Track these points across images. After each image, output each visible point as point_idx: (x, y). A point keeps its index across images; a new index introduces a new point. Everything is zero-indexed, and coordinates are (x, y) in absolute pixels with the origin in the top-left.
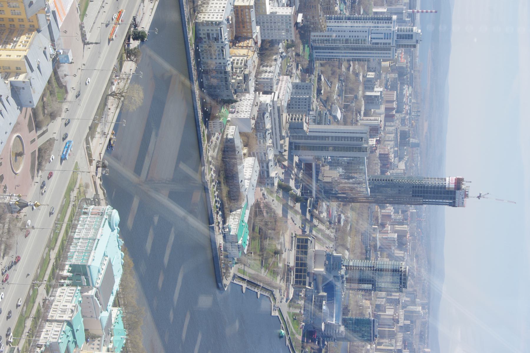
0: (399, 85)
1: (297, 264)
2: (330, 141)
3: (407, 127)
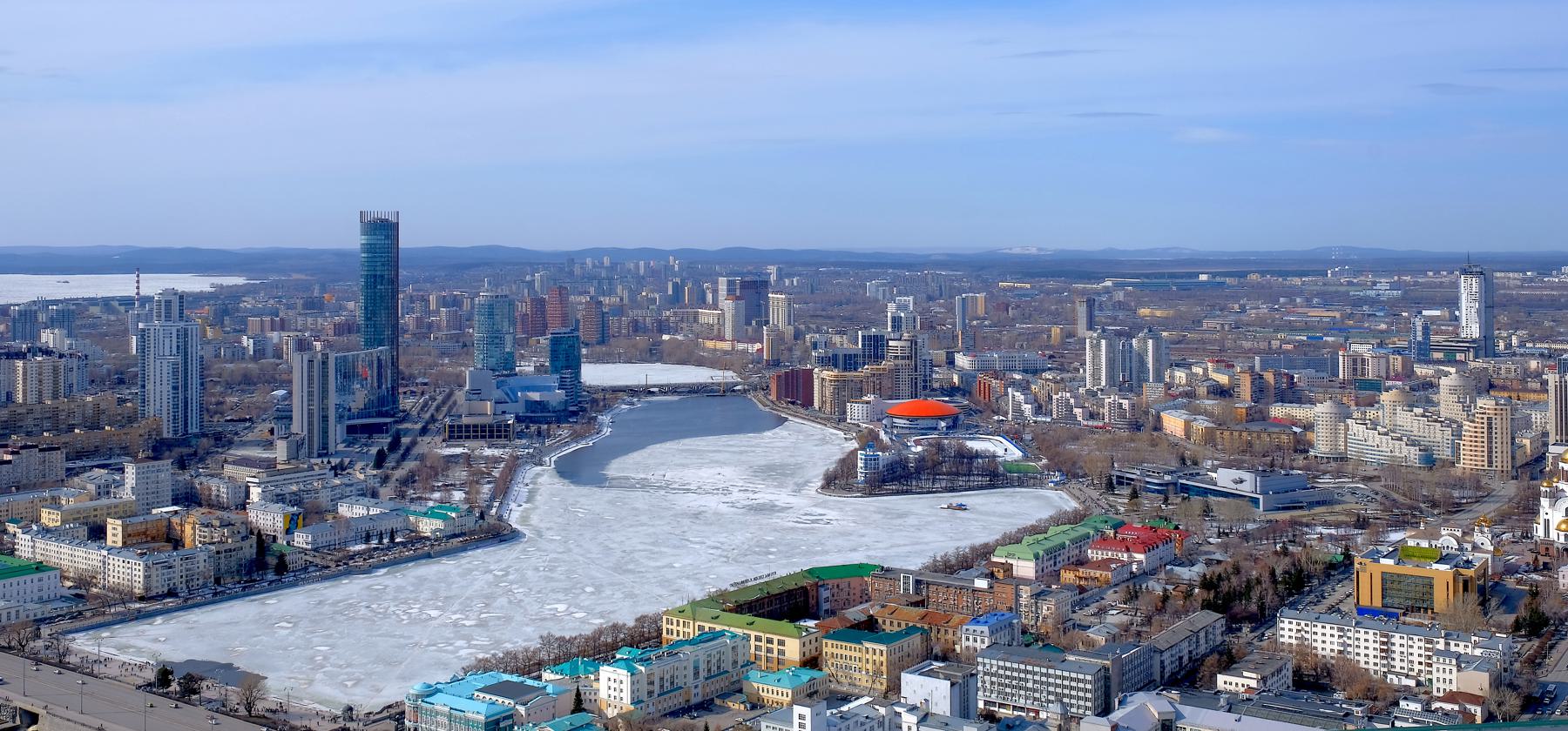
2: (315, 408)
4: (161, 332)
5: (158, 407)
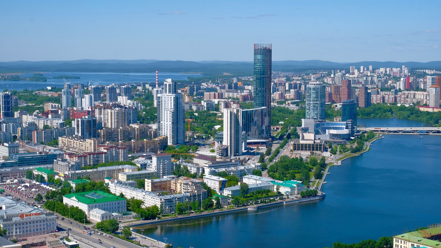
1: (309, 150)
4: (167, 98)
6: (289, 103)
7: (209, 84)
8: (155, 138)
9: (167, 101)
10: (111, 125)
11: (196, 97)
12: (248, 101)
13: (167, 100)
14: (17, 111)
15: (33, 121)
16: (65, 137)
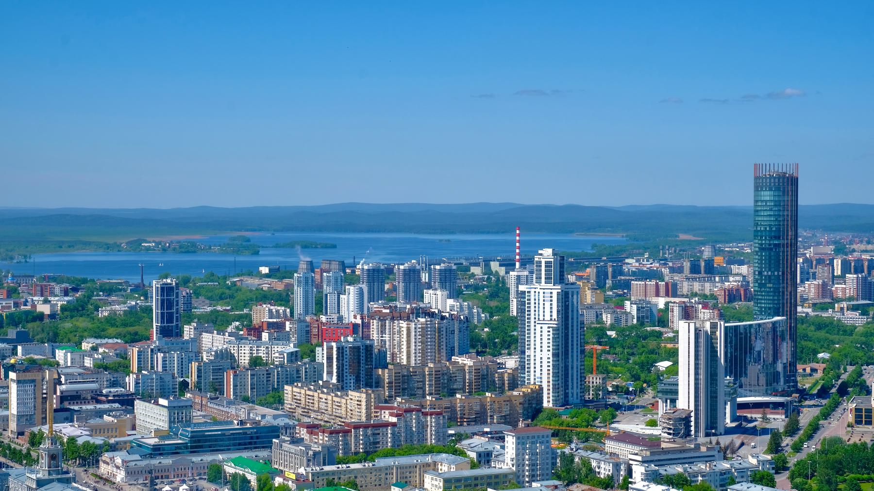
0: (623, 278)
3: (685, 263)
4: (541, 295)
5: (538, 374)
6: (842, 309)
7: (643, 261)
8: (513, 390)
9: (541, 302)
10: (409, 357)
11: (611, 293)
12: (740, 303)
13: (541, 299)
14: (189, 323)
15: (225, 346)
16: (300, 385)
